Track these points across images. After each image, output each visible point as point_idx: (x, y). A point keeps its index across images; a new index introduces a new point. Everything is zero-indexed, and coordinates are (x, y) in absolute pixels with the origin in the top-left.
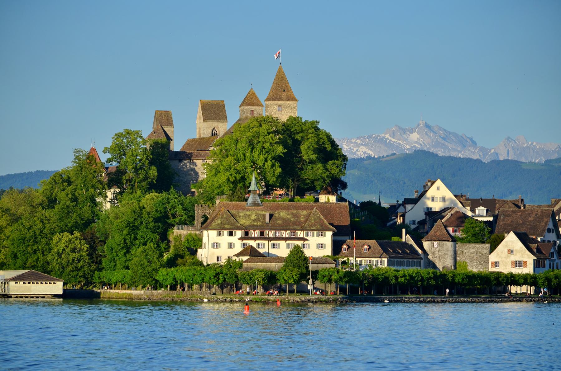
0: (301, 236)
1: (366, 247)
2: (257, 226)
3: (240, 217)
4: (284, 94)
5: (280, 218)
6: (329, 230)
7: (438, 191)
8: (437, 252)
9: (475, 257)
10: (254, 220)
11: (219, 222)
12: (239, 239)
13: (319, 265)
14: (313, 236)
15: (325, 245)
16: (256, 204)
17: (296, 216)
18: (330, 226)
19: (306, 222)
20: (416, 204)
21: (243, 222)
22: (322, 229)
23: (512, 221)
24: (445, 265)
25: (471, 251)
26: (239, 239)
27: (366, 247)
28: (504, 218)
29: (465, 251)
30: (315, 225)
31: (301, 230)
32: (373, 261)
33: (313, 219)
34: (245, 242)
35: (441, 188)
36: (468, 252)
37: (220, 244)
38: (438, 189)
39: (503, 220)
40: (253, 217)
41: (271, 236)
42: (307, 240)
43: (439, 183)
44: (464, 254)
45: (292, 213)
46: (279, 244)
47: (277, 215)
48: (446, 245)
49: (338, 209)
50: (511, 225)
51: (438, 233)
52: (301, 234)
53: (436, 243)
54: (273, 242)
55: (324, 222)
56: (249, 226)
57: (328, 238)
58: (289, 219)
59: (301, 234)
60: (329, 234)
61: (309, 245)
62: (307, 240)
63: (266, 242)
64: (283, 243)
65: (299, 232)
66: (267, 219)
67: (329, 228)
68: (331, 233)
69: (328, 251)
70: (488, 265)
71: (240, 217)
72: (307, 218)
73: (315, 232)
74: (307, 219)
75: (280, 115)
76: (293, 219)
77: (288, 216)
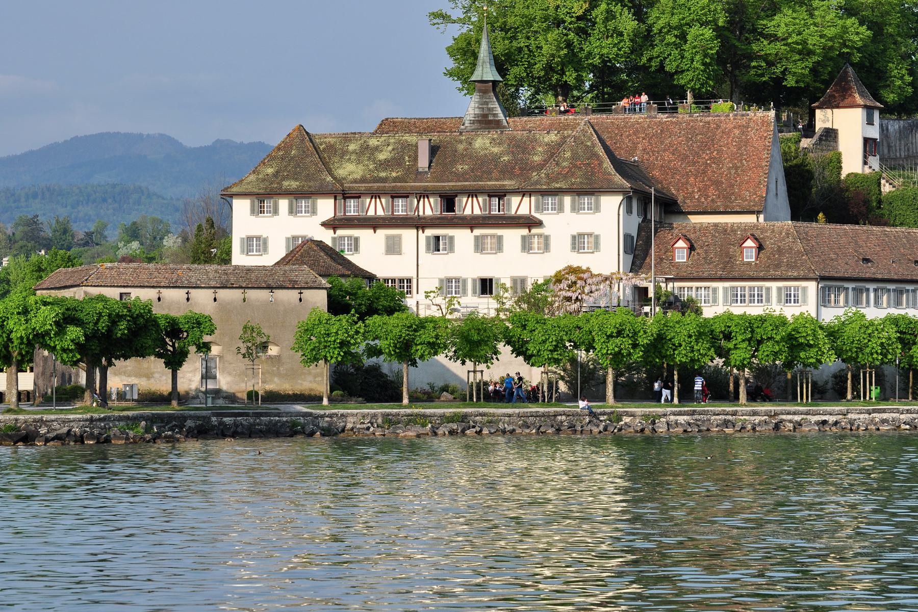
0: (524, 211)
1: (749, 243)
2: (384, 180)
3: (344, 153)
5: (469, 155)
6: (611, 190)
10: (385, 165)
11: (270, 171)
12: (325, 224)
13: (253, 294)
14: (561, 209)
15: (597, 237)
16: (490, 122)
17: (521, 147)
18: (618, 179)
19: (541, 166)
21: (349, 170)
22: (588, 190)
26: (325, 224)
27: (749, 243)
30: (565, 177)
31: (524, 193)
32: (768, 289)
33: (568, 154)
34: (340, 232)
37: (265, 241)
40: (382, 156)
41: (429, 212)
42: (539, 224)
45: (512, 139)
46: (451, 239)
47: (461, 147)
49: (737, 132)
52: (520, 206)
54: (430, 232)
55: (601, 164)
56: (363, 180)
57: (608, 218)
58: (495, 158)
59: (520, 206)
60: (611, 204)
61: (547, 238)
62: (539, 224)
63: (408, 235)
64: (463, 237)
65: (515, 200)
66: (423, 162)
67: (609, 181)
68: (621, 198)
69: (607, 259)
71: (344, 153)
72: (553, 151)
73: (567, 200)
74: (552, 155)
76: (506, 158)
77: (496, 150)
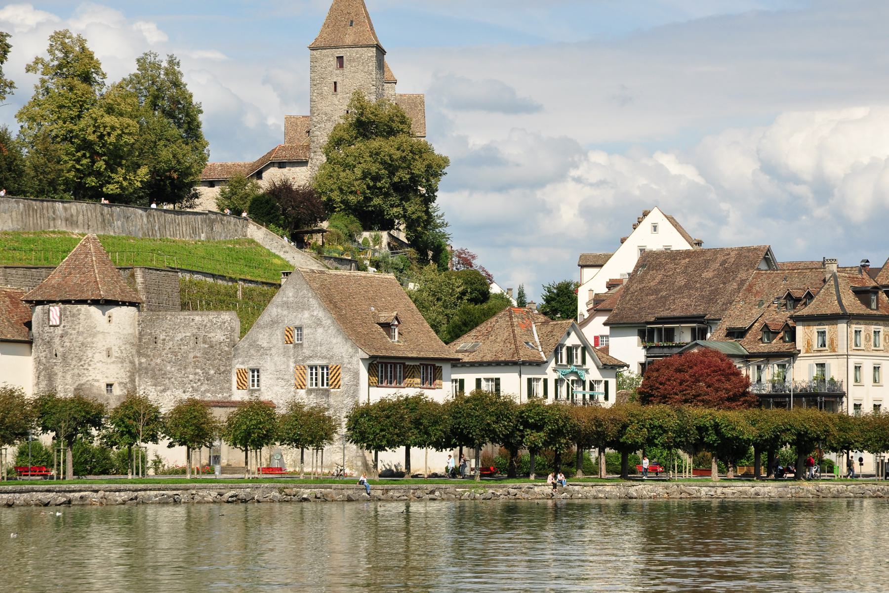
4: (350, 30)
7: (655, 235)
8: (57, 340)
9: (191, 355)
20: (601, 266)
23: (661, 282)
24: (83, 380)
25: (179, 336)
28: (646, 273)
29: (162, 337)
35: (659, 228)
36: (172, 339)
38: (655, 228)
39: (641, 280)
43: (655, 216)
44: (159, 345)
48: (88, 316)
50: (656, 291)
51: (76, 279)
53: (55, 311)
70: (229, 381)
75: (339, 80)
